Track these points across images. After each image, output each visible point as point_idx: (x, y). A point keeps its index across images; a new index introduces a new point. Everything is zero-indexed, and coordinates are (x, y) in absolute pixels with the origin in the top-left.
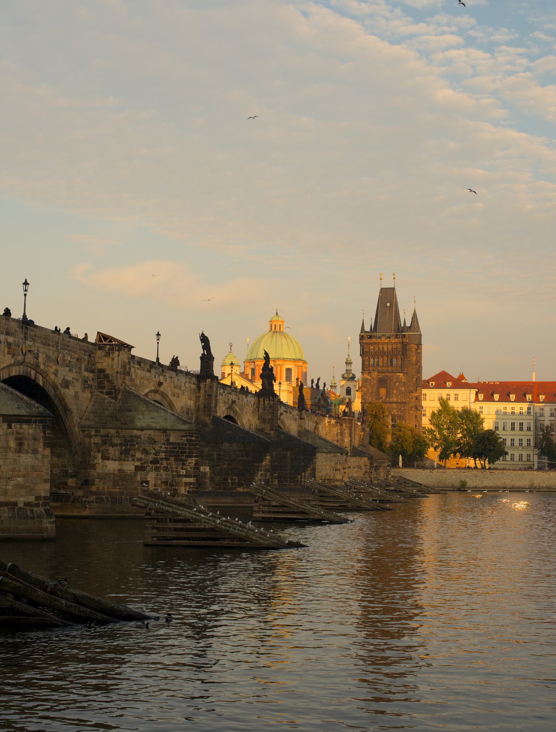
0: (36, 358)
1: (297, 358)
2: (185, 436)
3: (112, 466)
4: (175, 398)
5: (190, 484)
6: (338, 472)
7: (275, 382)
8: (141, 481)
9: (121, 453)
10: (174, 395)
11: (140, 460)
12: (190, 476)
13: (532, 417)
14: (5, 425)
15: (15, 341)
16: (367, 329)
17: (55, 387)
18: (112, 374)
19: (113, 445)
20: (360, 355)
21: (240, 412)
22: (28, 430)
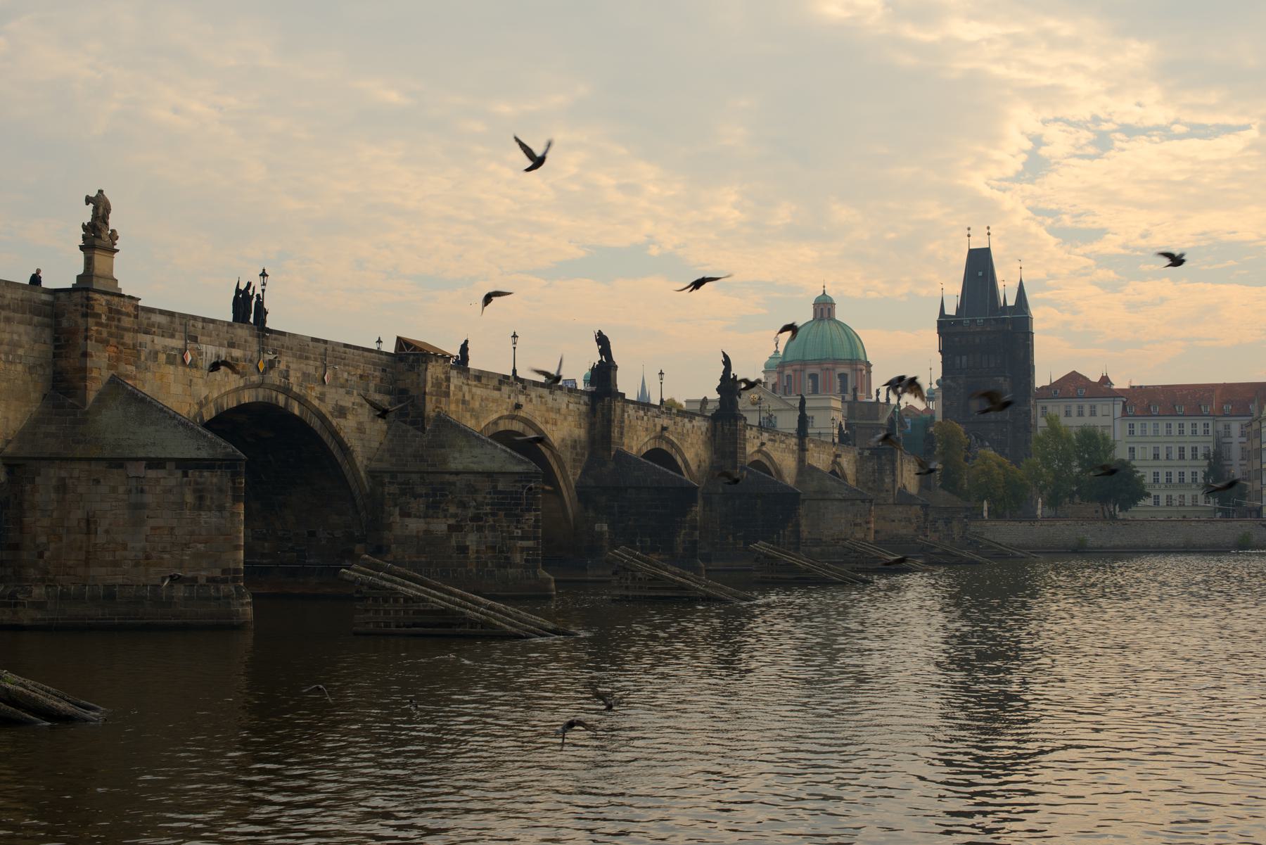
0: (284, 378)
1: (855, 358)
2: (521, 481)
3: (415, 525)
4: (548, 426)
5: (528, 549)
6: (859, 528)
7: (740, 398)
8: (457, 546)
9: (428, 507)
10: (547, 422)
11: (455, 516)
12: (528, 539)
13: (1211, 439)
14: (179, 473)
15: (245, 355)
16: (951, 310)
17: (322, 417)
18: (417, 396)
19: (416, 496)
20: (939, 351)
21: (679, 444)
22: (211, 479)
